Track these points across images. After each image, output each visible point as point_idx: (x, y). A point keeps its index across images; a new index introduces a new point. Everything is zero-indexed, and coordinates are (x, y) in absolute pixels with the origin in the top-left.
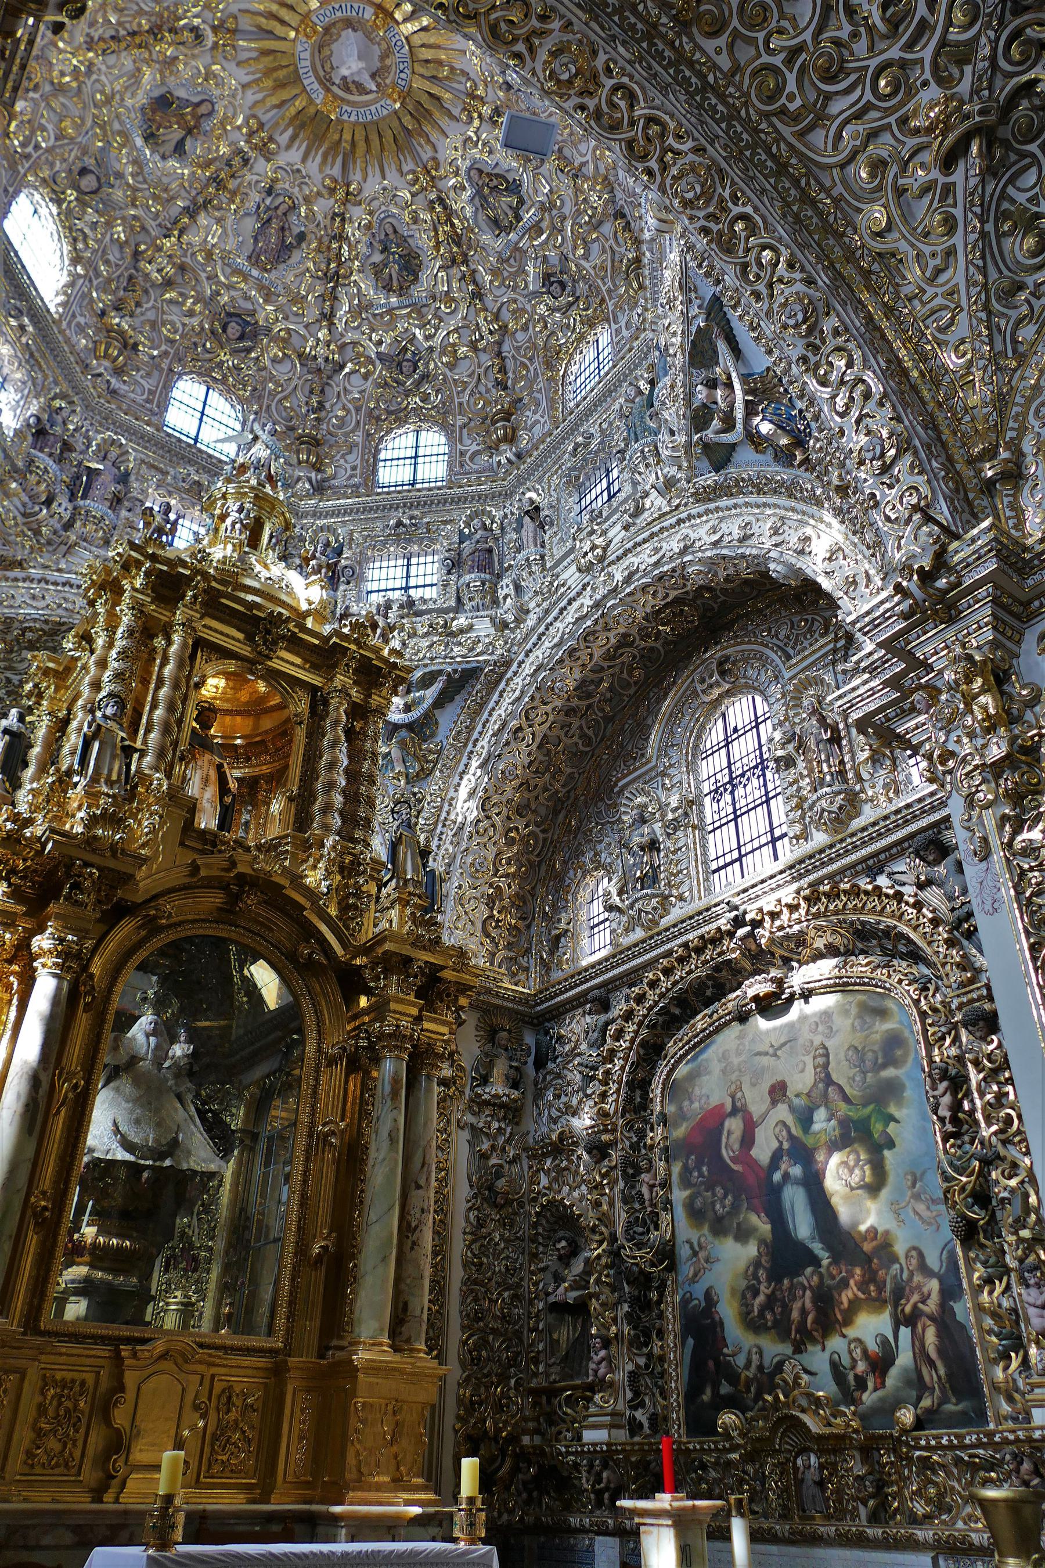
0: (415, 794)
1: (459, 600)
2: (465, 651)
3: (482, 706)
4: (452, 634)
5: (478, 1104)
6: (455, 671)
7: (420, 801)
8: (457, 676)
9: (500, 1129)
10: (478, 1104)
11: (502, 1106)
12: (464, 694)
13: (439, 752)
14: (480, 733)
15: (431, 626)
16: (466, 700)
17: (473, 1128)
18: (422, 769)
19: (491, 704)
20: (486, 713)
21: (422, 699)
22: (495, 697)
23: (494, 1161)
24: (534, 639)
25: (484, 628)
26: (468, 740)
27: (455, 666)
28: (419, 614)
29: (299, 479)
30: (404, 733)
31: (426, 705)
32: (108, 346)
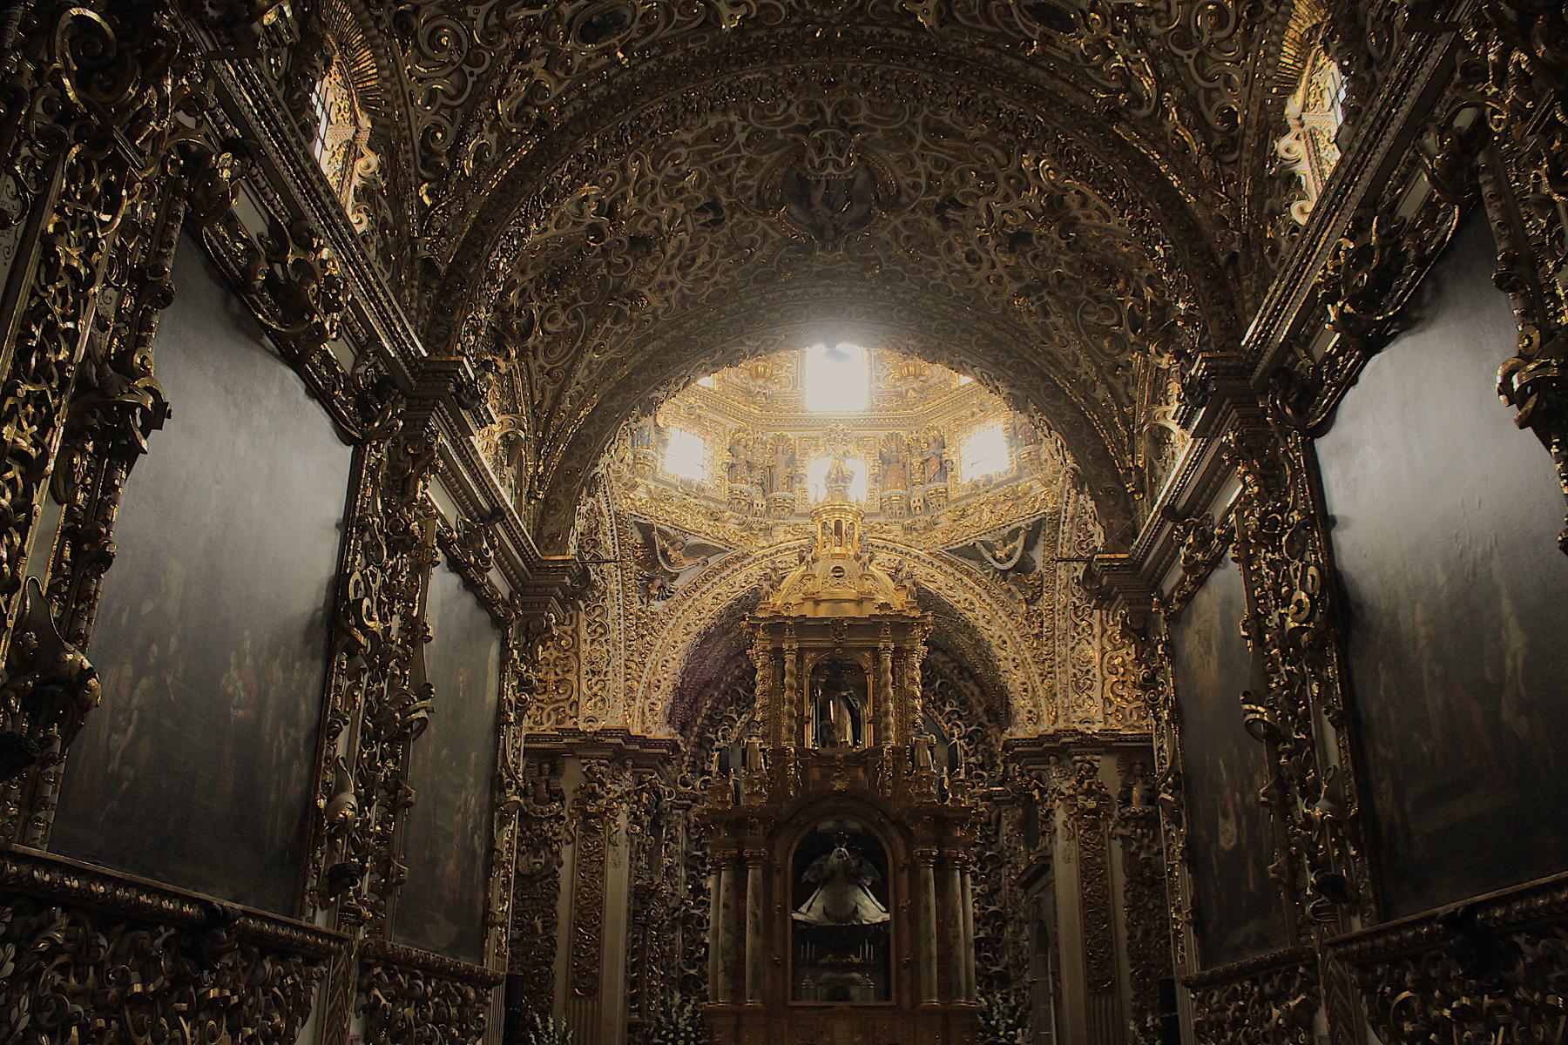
1: (1019, 468)
3: (1056, 542)
4: (1019, 498)
5: (1125, 820)
6: (1028, 526)
9: (1143, 834)
10: (1125, 820)
11: (1142, 818)
12: (1042, 537)
13: (1042, 578)
17: (1122, 836)
19: (1060, 541)
21: (1015, 548)
23: (1142, 855)
24: (1066, 495)
25: (1038, 488)
29: (907, 391)
30: (1011, 575)
32: (757, 367)
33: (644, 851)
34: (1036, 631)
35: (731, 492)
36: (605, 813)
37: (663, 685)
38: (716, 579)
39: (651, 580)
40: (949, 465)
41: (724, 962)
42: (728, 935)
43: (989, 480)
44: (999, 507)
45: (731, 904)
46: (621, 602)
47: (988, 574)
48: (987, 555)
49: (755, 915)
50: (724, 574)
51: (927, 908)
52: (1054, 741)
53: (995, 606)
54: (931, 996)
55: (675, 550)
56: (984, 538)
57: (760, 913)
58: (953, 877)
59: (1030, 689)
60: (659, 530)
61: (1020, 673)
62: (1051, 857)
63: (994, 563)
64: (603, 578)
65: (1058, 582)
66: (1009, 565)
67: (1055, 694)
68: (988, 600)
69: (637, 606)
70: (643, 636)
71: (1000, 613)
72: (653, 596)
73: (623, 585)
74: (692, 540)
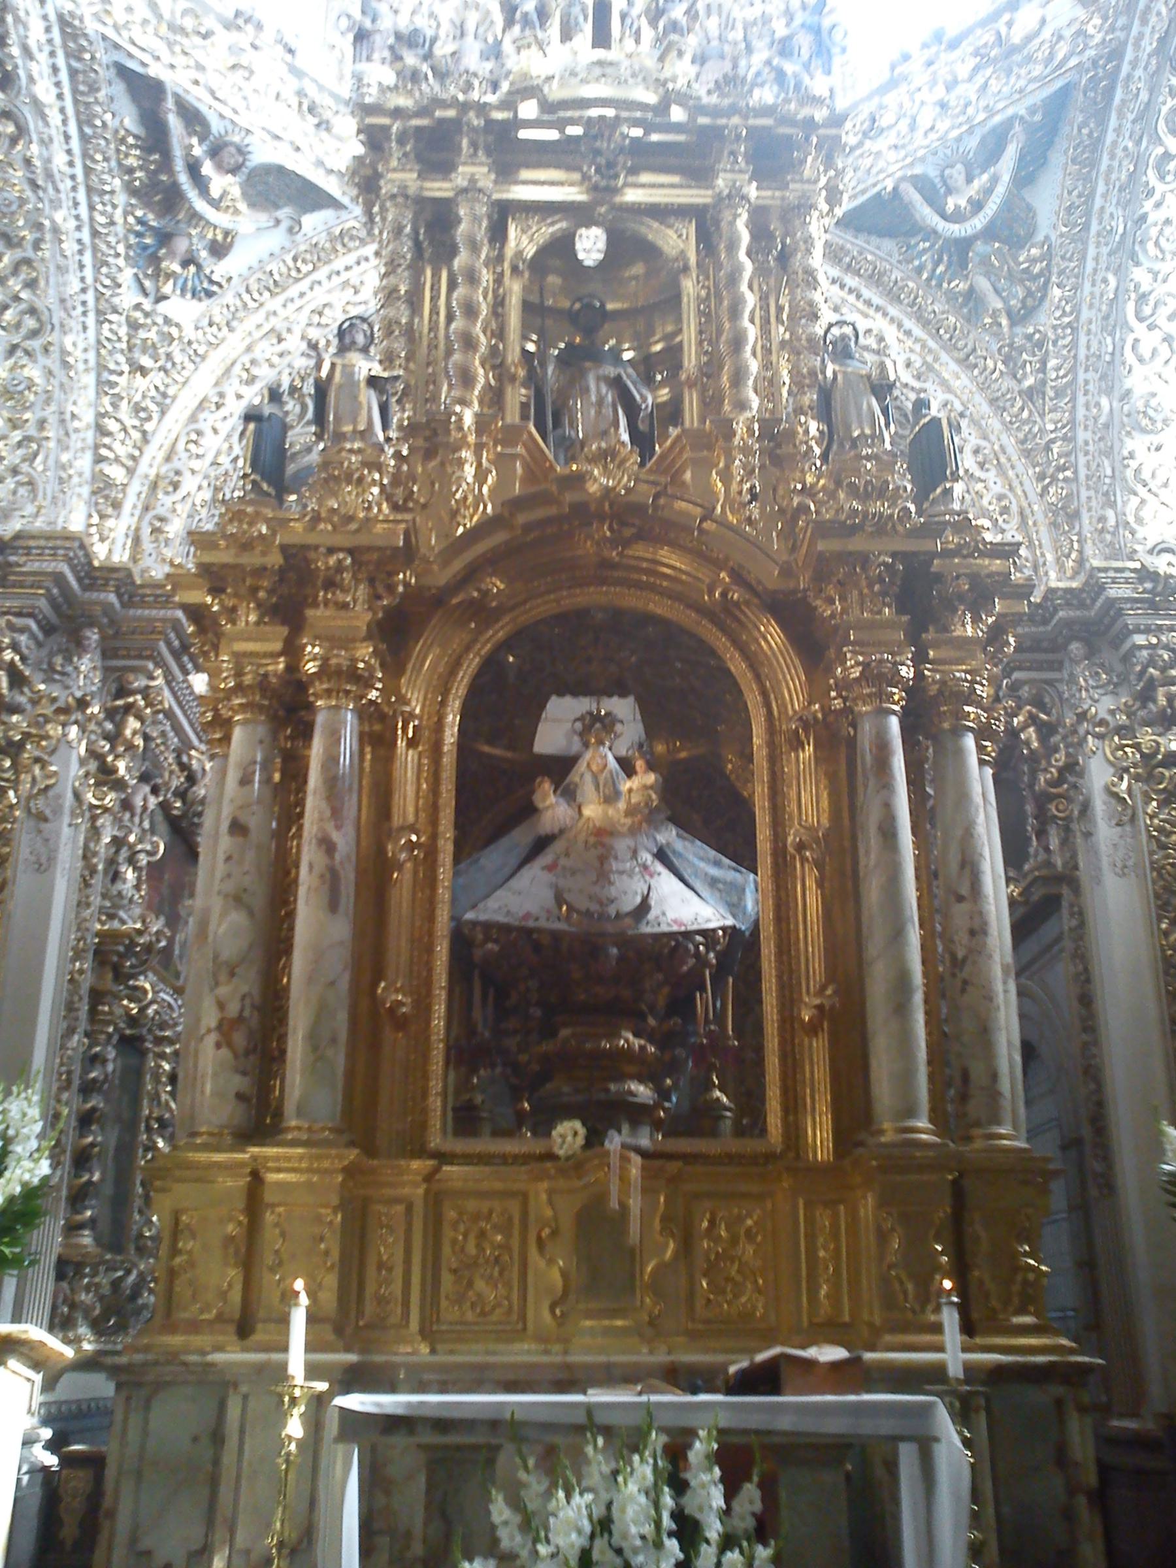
0: (1029, 337)
2: (1038, 70)
3: (1096, 144)
6: (1032, 111)
7: (1040, 345)
8: (1038, 117)
12: (1061, 143)
13: (1048, 256)
14: (1105, 196)
15: (976, 53)
16: (1066, 152)
18: (1029, 293)
19: (1110, 137)
20: (1105, 157)
22: (1113, 122)
26: (1088, 214)
27: (1029, 101)
28: (953, 45)
30: (979, 247)
31: (1000, 190)
33: (132, 861)
34: (1029, 382)
35: (359, 79)
36: (21, 746)
37: (189, 484)
38: (321, 274)
39: (165, 238)
40: (838, 35)
41: (221, 1006)
42: (238, 918)
43: (938, 37)
44: (960, 89)
45: (260, 823)
46: (88, 272)
47: (919, 270)
48: (927, 214)
49: (328, 846)
50: (339, 264)
51: (889, 833)
52: (1082, 605)
53: (931, 344)
54: (910, 1112)
55: (220, 167)
56: (918, 170)
57: (344, 840)
58: (960, 752)
59: (1014, 508)
60: (177, 96)
61: (991, 475)
62: (1069, 878)
63: (941, 225)
64: (34, 185)
65: (1092, 251)
66: (978, 223)
67: (1077, 515)
68: (918, 331)
69: (128, 297)
70: (144, 371)
71: (944, 357)
72: (170, 275)
73: (95, 234)
74: (262, 153)
